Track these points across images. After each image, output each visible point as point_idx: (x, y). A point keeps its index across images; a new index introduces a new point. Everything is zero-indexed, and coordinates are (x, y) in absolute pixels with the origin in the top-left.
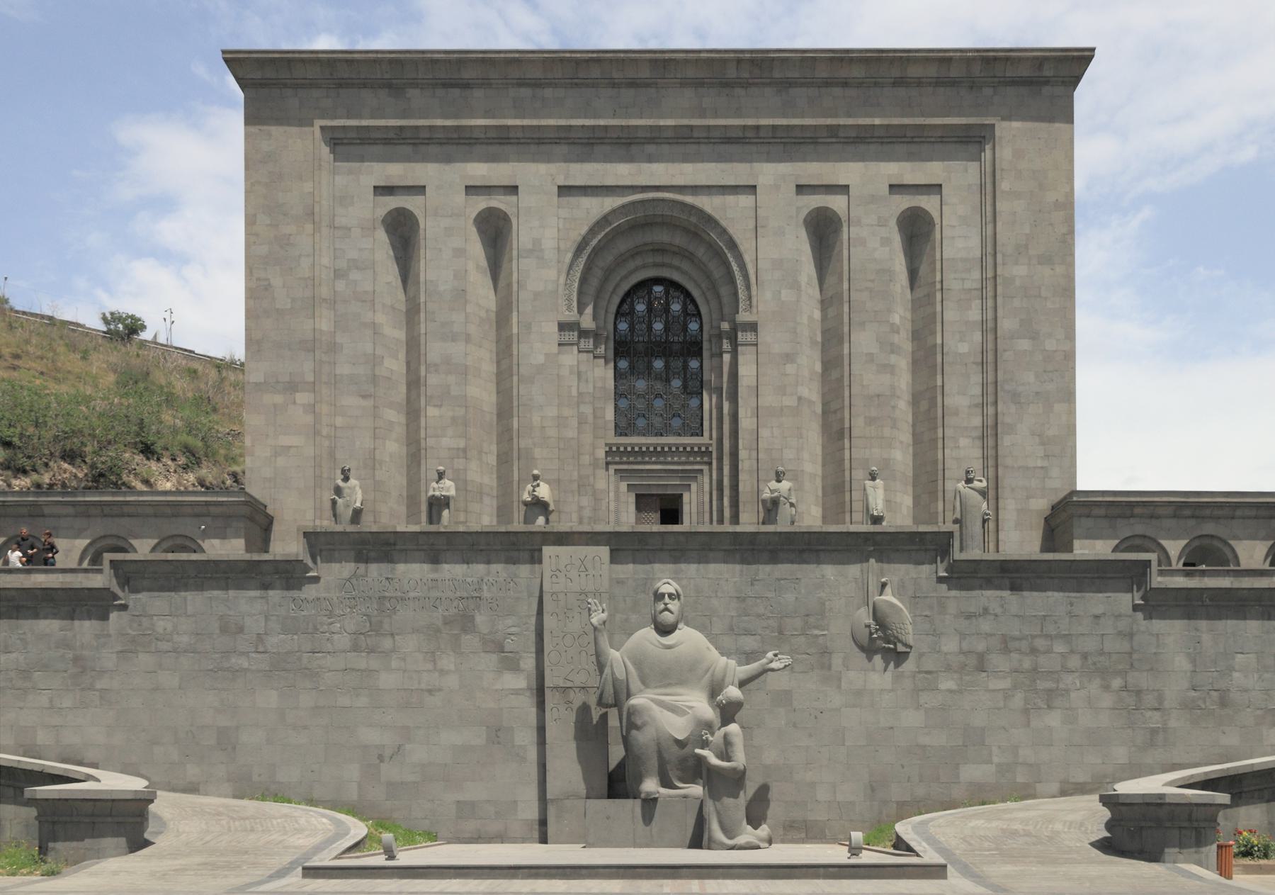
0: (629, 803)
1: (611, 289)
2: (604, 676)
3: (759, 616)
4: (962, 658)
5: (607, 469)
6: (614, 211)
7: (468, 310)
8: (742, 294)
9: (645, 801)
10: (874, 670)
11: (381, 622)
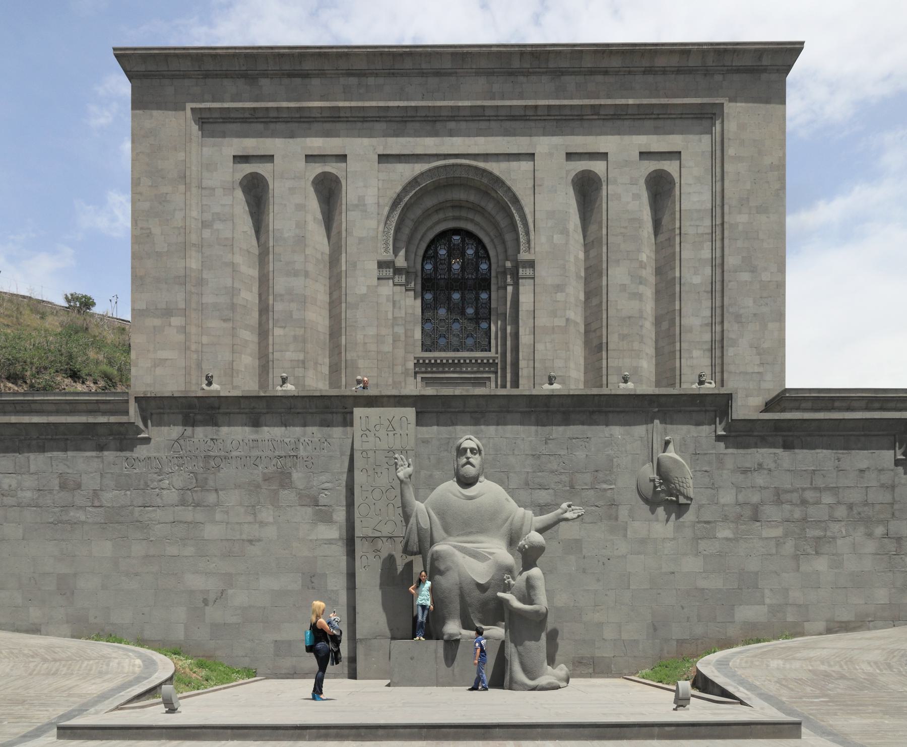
0: (433, 643)
1: (419, 237)
2: (409, 526)
3: (552, 472)
4: (738, 509)
5: (415, 378)
6: (422, 174)
7: (307, 252)
8: (522, 239)
9: (447, 642)
10: (657, 520)
11: (206, 479)
